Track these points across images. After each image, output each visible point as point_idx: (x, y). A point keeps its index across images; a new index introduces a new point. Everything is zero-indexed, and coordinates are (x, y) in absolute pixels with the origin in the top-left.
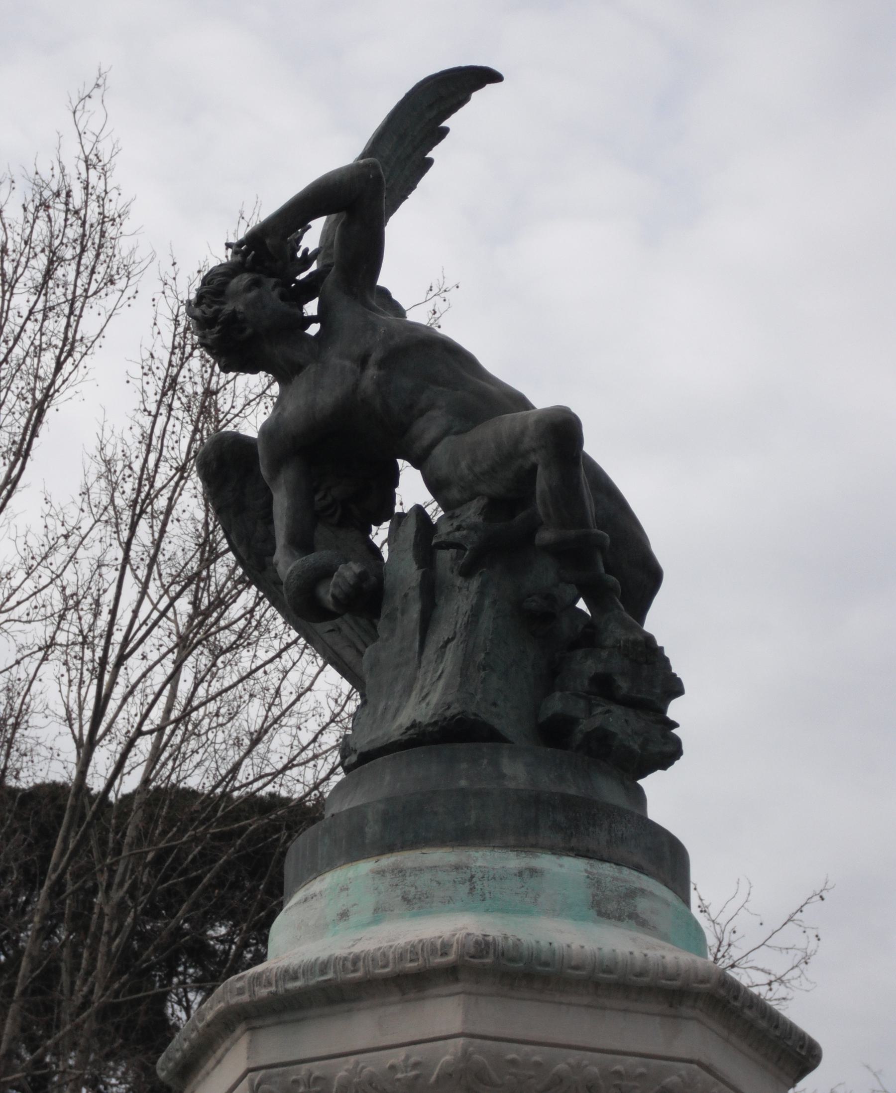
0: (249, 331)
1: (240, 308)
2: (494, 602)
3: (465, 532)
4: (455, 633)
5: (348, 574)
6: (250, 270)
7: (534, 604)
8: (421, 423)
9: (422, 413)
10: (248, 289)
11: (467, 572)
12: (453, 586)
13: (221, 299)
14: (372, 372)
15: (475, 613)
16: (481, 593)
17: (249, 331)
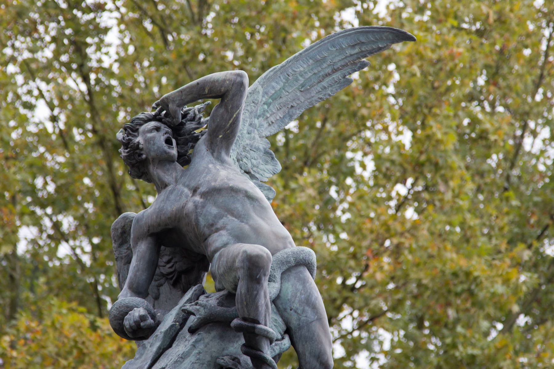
0: (144, 156)
1: (142, 142)
2: (199, 353)
3: (198, 307)
4: (167, 365)
5: (137, 314)
6: (160, 120)
7: (222, 361)
8: (215, 236)
9: (217, 230)
10: (150, 131)
11: (192, 331)
12: (185, 337)
13: (136, 134)
14: (197, 198)
15: (183, 357)
16: (194, 346)
17: (144, 156)
